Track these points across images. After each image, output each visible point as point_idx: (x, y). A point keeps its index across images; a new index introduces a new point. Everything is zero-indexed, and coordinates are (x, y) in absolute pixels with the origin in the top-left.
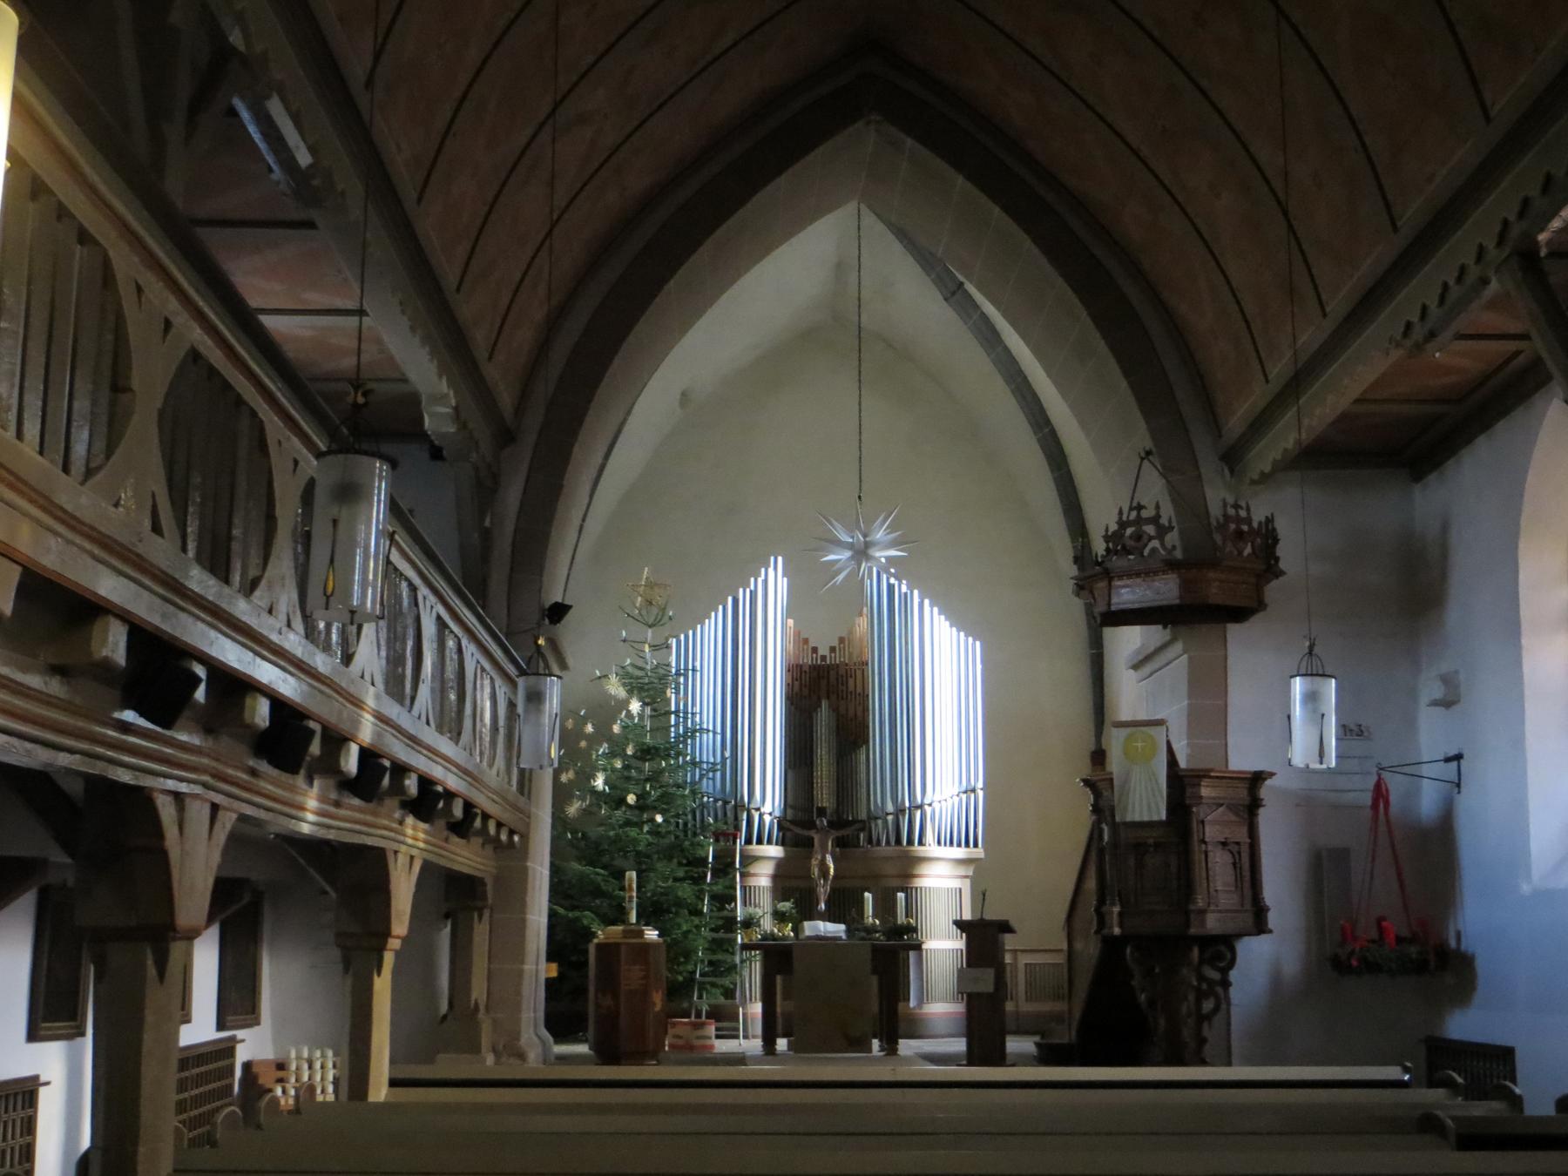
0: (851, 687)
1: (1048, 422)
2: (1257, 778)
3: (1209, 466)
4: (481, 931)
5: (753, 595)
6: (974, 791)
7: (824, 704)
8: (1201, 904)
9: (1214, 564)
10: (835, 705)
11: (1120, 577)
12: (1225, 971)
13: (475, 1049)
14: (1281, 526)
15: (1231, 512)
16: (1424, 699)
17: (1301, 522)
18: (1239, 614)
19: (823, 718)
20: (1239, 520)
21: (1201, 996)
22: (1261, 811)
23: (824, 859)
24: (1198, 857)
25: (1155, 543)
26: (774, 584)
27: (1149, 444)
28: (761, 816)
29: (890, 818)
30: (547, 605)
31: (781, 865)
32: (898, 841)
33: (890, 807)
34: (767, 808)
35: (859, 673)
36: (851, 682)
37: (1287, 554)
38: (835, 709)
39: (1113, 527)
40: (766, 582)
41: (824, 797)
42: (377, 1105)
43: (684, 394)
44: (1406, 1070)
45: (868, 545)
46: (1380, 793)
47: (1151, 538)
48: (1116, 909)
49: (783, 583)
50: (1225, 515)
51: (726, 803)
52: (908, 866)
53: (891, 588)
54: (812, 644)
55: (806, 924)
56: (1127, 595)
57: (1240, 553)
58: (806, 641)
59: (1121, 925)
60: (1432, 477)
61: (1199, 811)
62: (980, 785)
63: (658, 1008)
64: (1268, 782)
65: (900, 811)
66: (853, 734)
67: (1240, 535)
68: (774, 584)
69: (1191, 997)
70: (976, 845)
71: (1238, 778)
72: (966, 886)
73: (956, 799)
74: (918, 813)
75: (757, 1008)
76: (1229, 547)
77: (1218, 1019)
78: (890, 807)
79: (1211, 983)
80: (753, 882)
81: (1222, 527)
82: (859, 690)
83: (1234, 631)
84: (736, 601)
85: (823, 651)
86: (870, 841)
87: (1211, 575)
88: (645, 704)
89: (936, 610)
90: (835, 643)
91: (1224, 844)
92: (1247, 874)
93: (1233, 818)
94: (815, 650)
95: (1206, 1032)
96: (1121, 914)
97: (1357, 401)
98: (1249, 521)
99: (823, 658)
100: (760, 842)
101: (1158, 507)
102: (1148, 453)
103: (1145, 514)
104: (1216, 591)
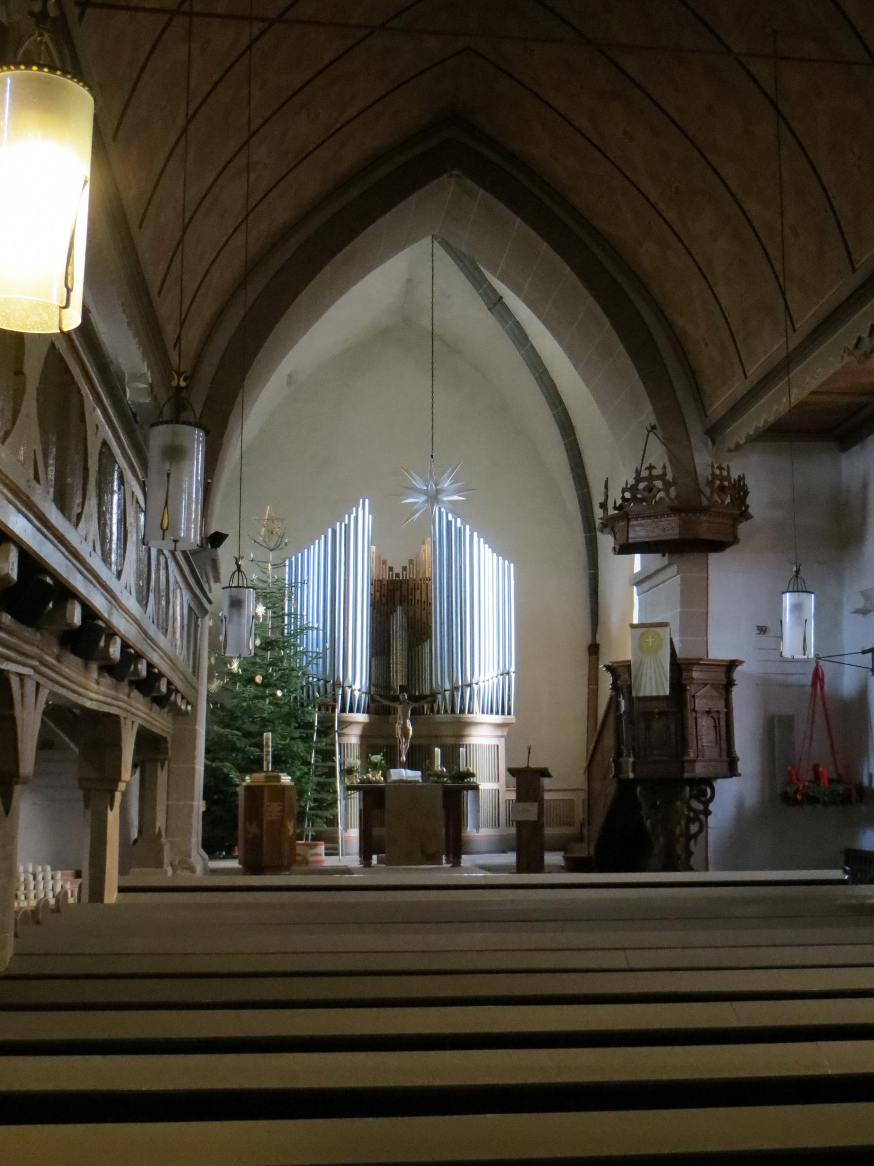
0: (418, 597)
1: (561, 402)
2: (732, 665)
3: (697, 436)
4: (162, 776)
5: (347, 527)
6: (508, 673)
7: (399, 609)
8: (692, 755)
9: (705, 510)
10: (405, 609)
11: (636, 518)
12: (707, 803)
13: (159, 864)
14: (749, 482)
15: (717, 472)
16: (847, 609)
17: (762, 477)
18: (718, 546)
19: (398, 619)
20: (722, 478)
21: (690, 821)
22: (735, 689)
23: (405, 724)
24: (691, 723)
25: (661, 494)
26: (362, 519)
27: (653, 421)
28: (352, 692)
29: (447, 694)
30: (209, 535)
31: (367, 727)
32: (453, 711)
33: (447, 686)
34: (357, 686)
35: (424, 587)
36: (418, 592)
37: (755, 502)
38: (406, 613)
39: (632, 482)
40: (356, 518)
41: (398, 679)
42: (110, 906)
43: (290, 376)
44: (846, 872)
45: (438, 492)
46: (818, 677)
47: (659, 490)
48: (631, 759)
49: (369, 519)
50: (713, 474)
51: (326, 682)
52: (460, 727)
53: (449, 523)
54: (389, 565)
55: (392, 771)
56: (639, 532)
57: (723, 502)
58: (384, 562)
59: (634, 771)
60: (856, 448)
61: (691, 689)
62: (513, 669)
63: (291, 833)
64: (739, 668)
65: (455, 688)
66: (419, 632)
67: (722, 489)
68: (362, 519)
69: (683, 822)
70: (509, 713)
71: (715, 665)
72: (502, 743)
73: (495, 680)
74: (468, 690)
75: (354, 833)
76: (716, 497)
77: (701, 838)
78: (447, 686)
79: (697, 812)
81: (710, 483)
82: (424, 599)
83: (714, 558)
84: (334, 532)
85: (398, 570)
86: (432, 710)
87: (703, 518)
88: (268, 608)
89: (482, 540)
90: (407, 564)
91: (708, 712)
92: (724, 737)
93: (714, 693)
94: (391, 569)
95: (692, 846)
96: (634, 763)
97: (813, 393)
98: (728, 478)
99: (397, 575)
100: (351, 711)
101: (664, 467)
102: (653, 428)
103: (655, 472)
104: (705, 529)
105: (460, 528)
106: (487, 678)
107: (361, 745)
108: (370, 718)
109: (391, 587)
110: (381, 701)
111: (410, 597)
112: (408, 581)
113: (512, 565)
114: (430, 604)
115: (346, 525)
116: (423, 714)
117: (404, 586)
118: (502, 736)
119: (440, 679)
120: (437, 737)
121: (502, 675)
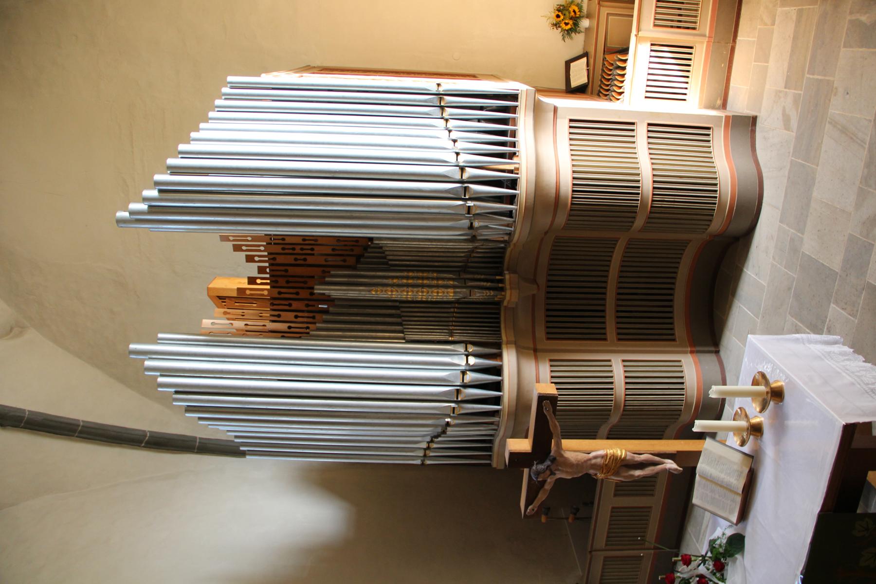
6: (440, 96)
28: (466, 386)
65: (463, 194)
73: (452, 124)
85: (252, 269)
99: (261, 270)
105: (160, 191)
109: (282, 282)
110: (481, 326)
111: (298, 251)
112: (269, 254)
113: (230, 79)
115: (177, 392)
117: (280, 259)
119: (449, 234)
121: (442, 108)
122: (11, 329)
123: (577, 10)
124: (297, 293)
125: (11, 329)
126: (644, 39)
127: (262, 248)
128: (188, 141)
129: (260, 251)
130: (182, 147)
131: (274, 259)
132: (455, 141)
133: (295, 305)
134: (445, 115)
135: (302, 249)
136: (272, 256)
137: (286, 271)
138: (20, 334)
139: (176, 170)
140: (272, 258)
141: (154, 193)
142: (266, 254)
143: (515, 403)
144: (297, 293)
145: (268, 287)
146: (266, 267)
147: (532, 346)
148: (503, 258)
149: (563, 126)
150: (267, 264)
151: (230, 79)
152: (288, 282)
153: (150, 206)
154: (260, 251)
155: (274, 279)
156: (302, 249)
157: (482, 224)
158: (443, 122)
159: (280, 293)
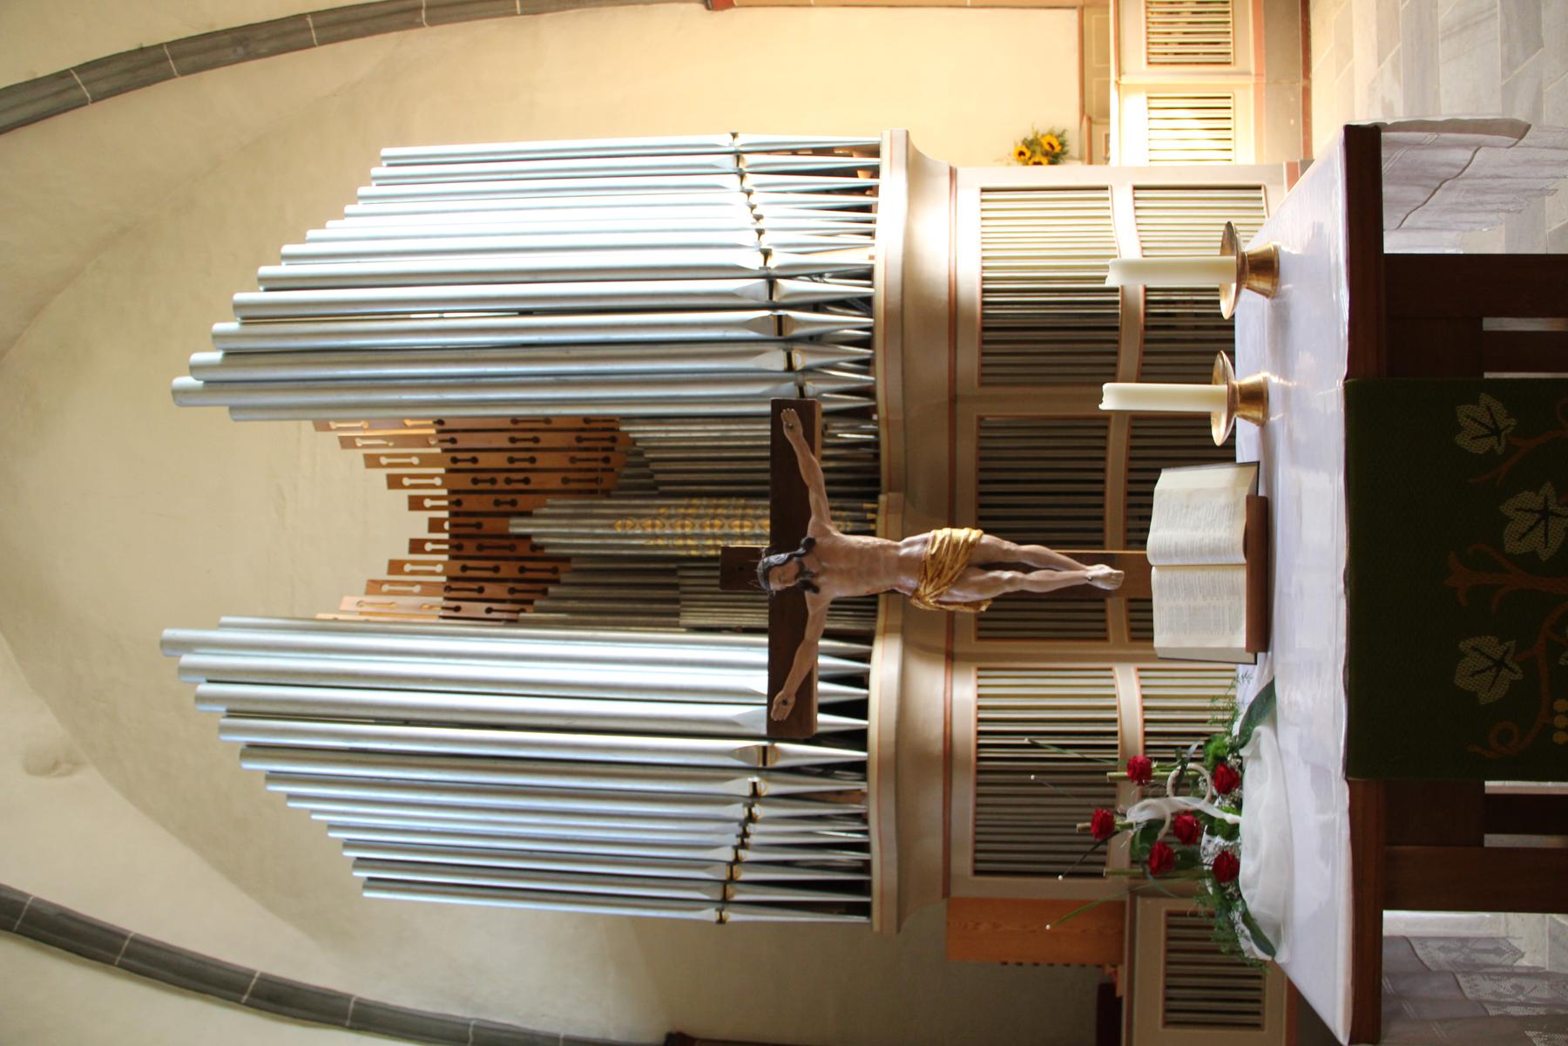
0: (499, 461)
6: (738, 155)
7: (518, 527)
19: (552, 529)
29: (800, 361)
36: (486, 461)
54: (403, 553)
58: (396, 566)
66: (604, 459)
74: (786, 285)
78: (774, 360)
80: (966, 729)
82: (501, 441)
85: (418, 526)
86: (864, 414)
94: (416, 546)
99: (435, 525)
100: (859, 708)
106: (747, 219)
107: (985, 665)
108: (888, 631)
109: (470, 547)
111: (501, 485)
112: (452, 492)
113: (386, 152)
114: (587, 419)
115: (232, 714)
116: (875, 445)
117: (470, 503)
118: (953, 174)
120: (953, 400)
122: (56, 765)
123: (1055, 143)
124: (496, 569)
125: (56, 765)
126: (1136, 88)
127: (438, 481)
128: (303, 241)
129: (433, 486)
130: (288, 249)
131: (458, 503)
132: (758, 218)
133: (491, 590)
134: (748, 184)
135: (508, 481)
136: (455, 498)
137: (479, 526)
138: (69, 773)
139: (273, 284)
140: (456, 499)
141: (233, 326)
142: (444, 492)
143: (892, 738)
144: (496, 569)
145: (445, 557)
146: (443, 520)
147: (942, 643)
148: (877, 470)
149: (969, 196)
150: (445, 514)
151: (386, 152)
152: (480, 547)
153: (229, 354)
154: (433, 486)
155: (456, 542)
156: (508, 481)
157: (811, 361)
158: (736, 178)
159: (464, 568)
